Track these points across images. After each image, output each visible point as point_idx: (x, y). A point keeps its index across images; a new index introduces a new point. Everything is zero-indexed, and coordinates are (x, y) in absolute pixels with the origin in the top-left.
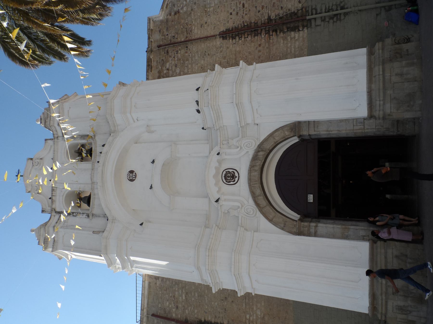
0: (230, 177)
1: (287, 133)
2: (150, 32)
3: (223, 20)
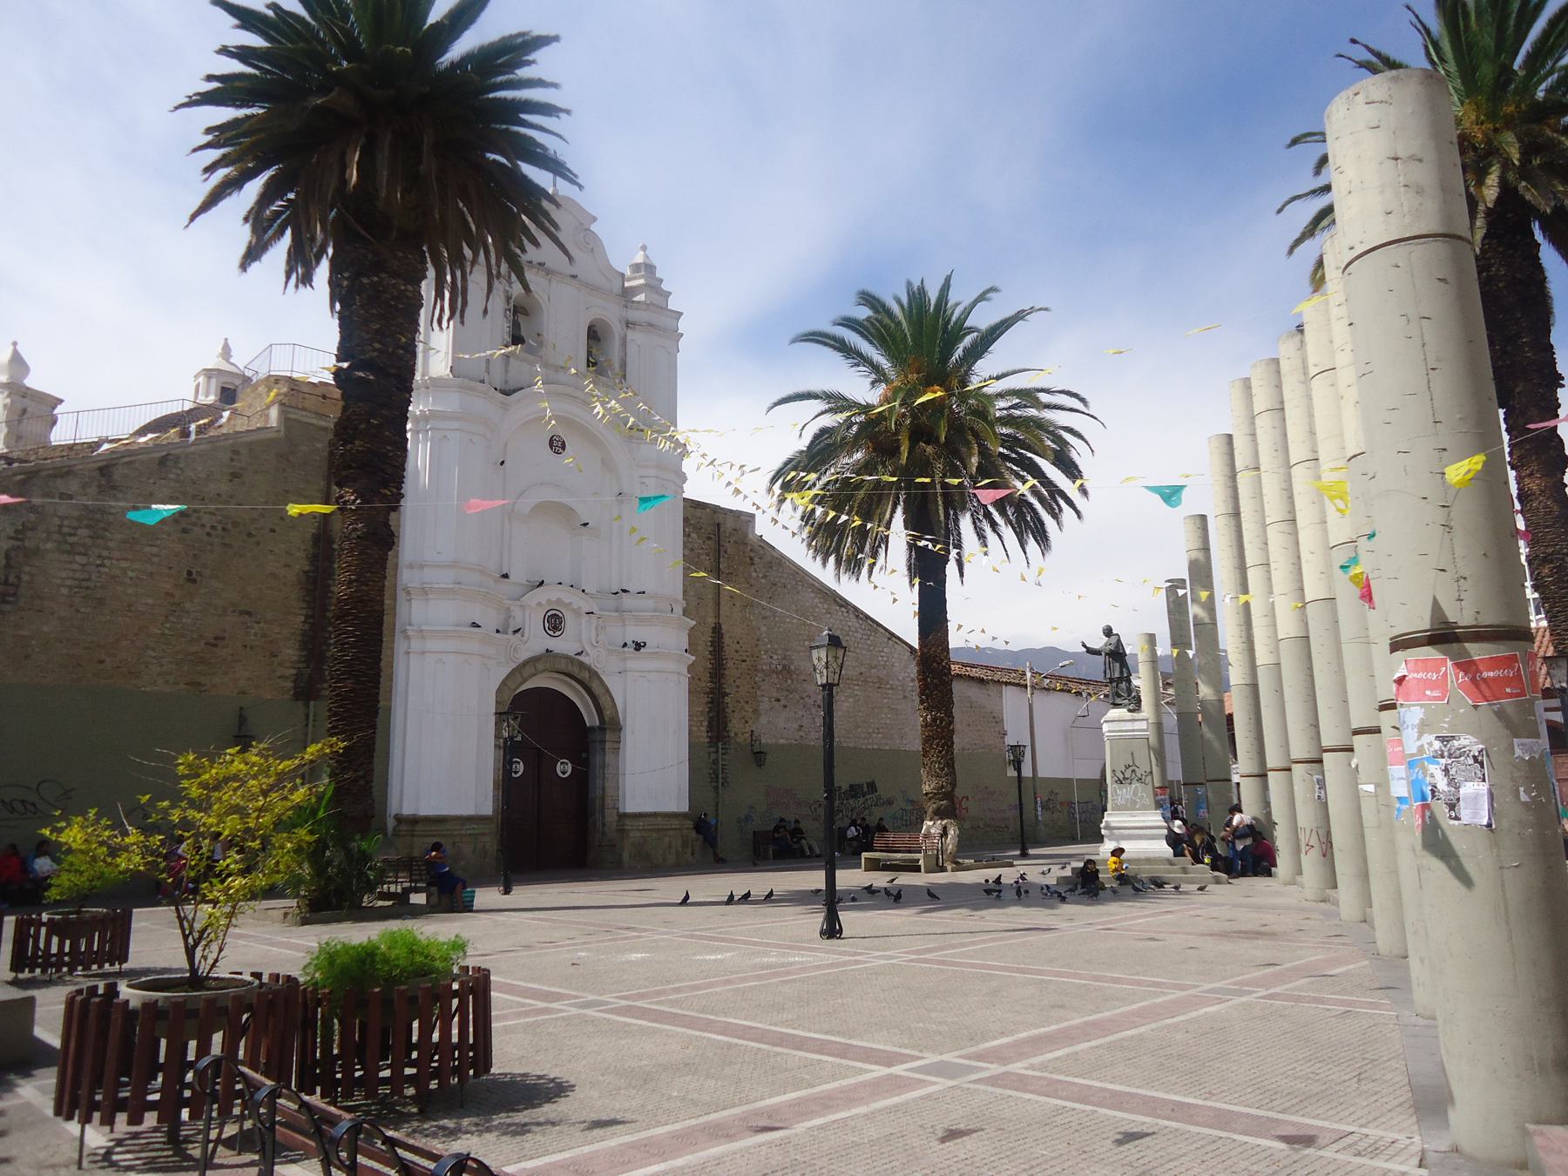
0: (554, 623)
1: (607, 713)
2: (737, 515)
3: (733, 631)
